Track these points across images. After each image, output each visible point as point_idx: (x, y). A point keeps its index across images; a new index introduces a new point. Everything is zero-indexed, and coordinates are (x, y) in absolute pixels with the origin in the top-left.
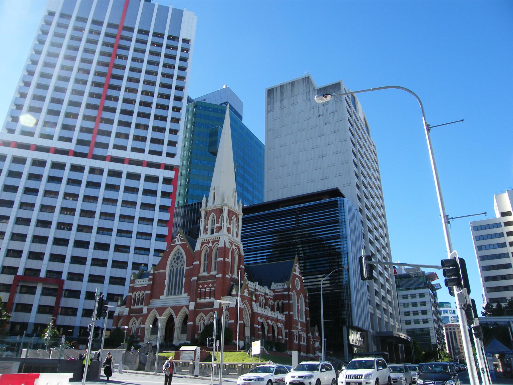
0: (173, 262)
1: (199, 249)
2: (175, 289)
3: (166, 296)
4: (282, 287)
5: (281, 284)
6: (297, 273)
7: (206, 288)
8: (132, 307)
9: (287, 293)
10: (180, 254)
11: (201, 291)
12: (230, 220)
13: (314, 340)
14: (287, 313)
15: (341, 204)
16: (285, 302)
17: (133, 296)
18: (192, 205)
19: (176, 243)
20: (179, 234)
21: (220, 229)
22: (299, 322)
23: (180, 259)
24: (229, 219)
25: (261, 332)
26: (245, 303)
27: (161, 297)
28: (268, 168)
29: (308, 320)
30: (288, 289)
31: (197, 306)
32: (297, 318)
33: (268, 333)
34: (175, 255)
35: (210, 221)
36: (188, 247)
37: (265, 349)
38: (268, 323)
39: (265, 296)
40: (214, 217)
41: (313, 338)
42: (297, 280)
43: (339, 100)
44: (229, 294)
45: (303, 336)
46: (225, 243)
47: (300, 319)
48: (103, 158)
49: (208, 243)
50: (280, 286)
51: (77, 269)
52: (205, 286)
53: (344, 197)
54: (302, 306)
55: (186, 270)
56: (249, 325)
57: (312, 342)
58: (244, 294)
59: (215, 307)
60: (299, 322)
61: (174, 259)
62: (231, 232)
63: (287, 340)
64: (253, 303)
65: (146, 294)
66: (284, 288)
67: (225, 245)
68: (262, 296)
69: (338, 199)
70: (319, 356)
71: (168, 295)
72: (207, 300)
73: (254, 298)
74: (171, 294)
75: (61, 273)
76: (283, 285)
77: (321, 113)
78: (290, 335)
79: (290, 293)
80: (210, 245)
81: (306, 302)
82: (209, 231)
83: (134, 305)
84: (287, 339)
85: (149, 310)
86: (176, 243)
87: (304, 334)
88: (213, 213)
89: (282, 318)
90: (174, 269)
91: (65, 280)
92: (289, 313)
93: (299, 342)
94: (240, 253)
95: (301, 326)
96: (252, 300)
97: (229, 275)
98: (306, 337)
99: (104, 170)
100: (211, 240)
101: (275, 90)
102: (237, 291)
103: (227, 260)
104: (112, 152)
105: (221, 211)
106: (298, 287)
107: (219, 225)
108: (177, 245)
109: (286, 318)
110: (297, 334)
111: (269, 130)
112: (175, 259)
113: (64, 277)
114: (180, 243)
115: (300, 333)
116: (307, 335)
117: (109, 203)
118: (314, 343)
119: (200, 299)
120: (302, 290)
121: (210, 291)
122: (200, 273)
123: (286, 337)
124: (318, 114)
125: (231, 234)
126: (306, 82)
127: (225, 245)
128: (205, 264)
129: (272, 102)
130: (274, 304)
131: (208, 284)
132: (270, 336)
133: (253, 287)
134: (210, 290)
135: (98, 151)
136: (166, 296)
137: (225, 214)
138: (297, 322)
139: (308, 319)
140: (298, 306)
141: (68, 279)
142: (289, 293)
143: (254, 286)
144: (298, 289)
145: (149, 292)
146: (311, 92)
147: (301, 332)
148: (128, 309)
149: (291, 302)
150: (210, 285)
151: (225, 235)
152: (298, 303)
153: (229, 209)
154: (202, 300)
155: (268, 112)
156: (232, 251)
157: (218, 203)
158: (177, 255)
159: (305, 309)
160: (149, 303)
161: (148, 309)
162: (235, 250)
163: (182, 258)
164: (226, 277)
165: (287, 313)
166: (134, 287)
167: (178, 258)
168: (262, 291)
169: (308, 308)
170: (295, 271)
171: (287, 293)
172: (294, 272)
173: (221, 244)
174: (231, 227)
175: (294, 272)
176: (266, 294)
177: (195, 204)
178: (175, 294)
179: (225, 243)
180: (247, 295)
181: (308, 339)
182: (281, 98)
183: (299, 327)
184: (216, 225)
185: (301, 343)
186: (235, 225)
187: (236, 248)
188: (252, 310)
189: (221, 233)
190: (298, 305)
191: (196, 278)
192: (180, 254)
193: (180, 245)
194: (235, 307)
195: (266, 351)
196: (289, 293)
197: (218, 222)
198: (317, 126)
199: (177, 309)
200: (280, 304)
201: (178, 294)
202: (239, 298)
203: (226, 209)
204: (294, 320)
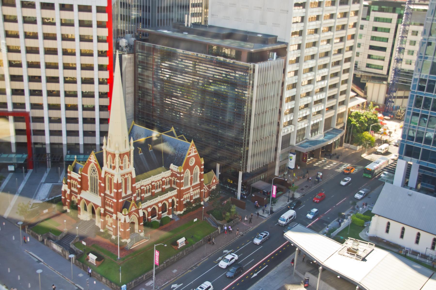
12: (122, 160)
24: (121, 160)
34: (92, 167)
46: (117, 180)
51: (36, 100)
67: (117, 182)
80: (110, 176)
82: (109, 166)
84: (178, 205)
86: (92, 161)
102: (125, 213)
113: (28, 109)
123: (177, 203)
127: (117, 182)
128: (108, 185)
130: (171, 179)
137: (117, 159)
140: (191, 177)
167: (94, 171)
174: (123, 165)
179: (117, 180)
180: (135, 209)
186: (127, 159)
188: (139, 215)
197: (113, 163)
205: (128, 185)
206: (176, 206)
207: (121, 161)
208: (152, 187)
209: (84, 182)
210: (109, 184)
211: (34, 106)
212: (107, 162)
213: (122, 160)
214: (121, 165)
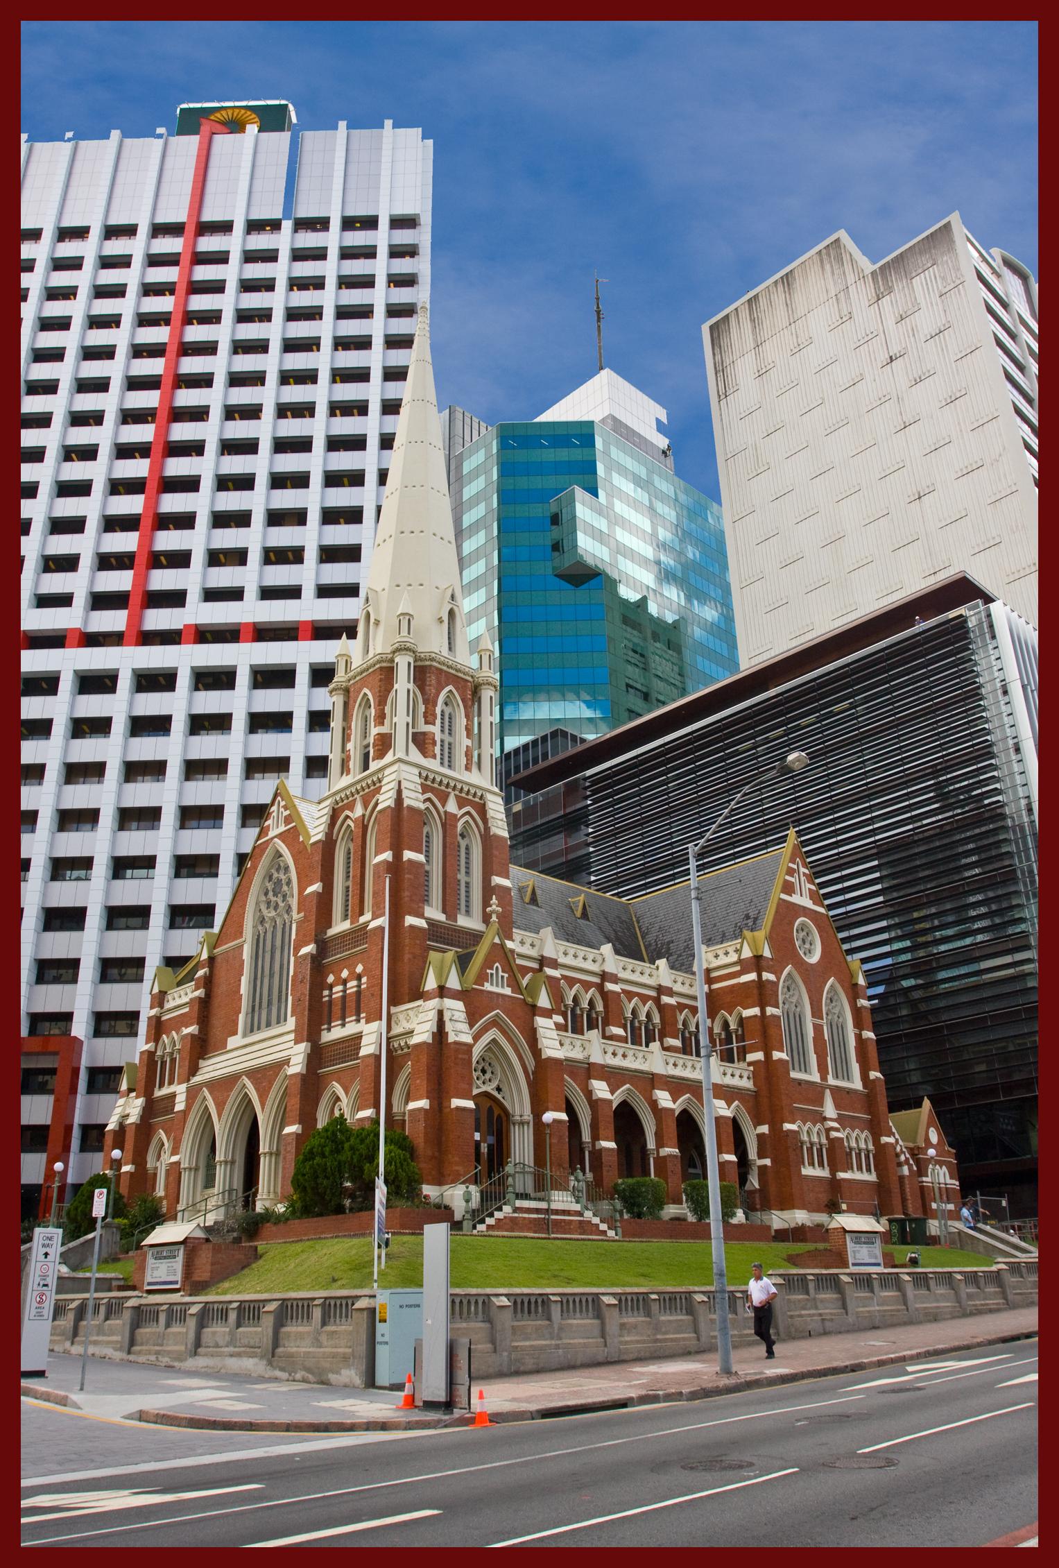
0: (263, 907)
1: (320, 837)
2: (270, 1003)
3: (245, 1036)
4: (733, 957)
5: (731, 945)
6: (802, 899)
7: (345, 982)
8: (158, 1093)
9: (752, 976)
10: (282, 872)
11: (330, 996)
13: (917, 1162)
14: (759, 1056)
15: (980, 624)
16: (747, 1013)
17: (159, 1053)
18: (517, 751)
19: (271, 834)
20: (279, 798)
21: (385, 743)
22: (828, 1092)
23: (285, 888)
24: (426, 702)
25: (612, 1145)
26: (494, 1023)
27: (233, 1042)
28: (741, 582)
29: (874, 1081)
30: (757, 963)
31: (317, 1056)
32: (815, 1077)
33: (660, 1144)
35: (356, 725)
36: (301, 839)
37: (588, 1214)
38: (654, 1104)
39: (657, 1001)
40: (370, 707)
41: (911, 1150)
42: (803, 927)
43: (953, 285)
44: (418, 994)
45: (846, 1144)
46: (399, 792)
47: (830, 1077)
48: (169, 637)
49: (351, 807)
50: (727, 953)
51: (118, 997)
52: (345, 974)
53: (988, 599)
54: (843, 1028)
55: (300, 924)
56: (528, 1115)
57: (910, 1169)
58: (488, 987)
59: (363, 1052)
60: (828, 1092)
61: (266, 894)
62: (437, 750)
63: (765, 1166)
64: (540, 1021)
65: (184, 1038)
66: (740, 962)
67: (399, 799)
68: (645, 999)
69: (970, 612)
70: (845, 1231)
71: (252, 1031)
72: (351, 1028)
73: (544, 1001)
74: (259, 1029)
75: (67, 1017)
76: (736, 951)
77: (894, 350)
78: (778, 1145)
79: (767, 976)
81: (857, 1012)
82: (356, 763)
83: (161, 1085)
84: (767, 1162)
85: (192, 1094)
87: (859, 1139)
88: (366, 690)
89: (736, 1082)
90: (265, 933)
91: (82, 1038)
92: (768, 1056)
93: (833, 1171)
94: (487, 829)
95: (837, 1107)
96: (534, 1010)
97: (420, 915)
98: (871, 1147)
99: (176, 675)
100: (361, 793)
101: (733, 320)
102: (442, 975)
103: (408, 855)
104: (198, 612)
105: (386, 674)
106: (809, 952)
107: (384, 729)
108: (272, 839)
109: (755, 1076)
110: (824, 1141)
111: (729, 456)
112: (271, 894)
113: (80, 1028)
114: (282, 828)
115: (834, 1134)
116: (876, 1142)
117: (207, 777)
118: (921, 1172)
119: (329, 1030)
120: (833, 963)
121: (359, 993)
122: (330, 927)
123: (761, 1156)
124: (887, 356)
125: (434, 757)
126: (831, 262)
127: (399, 799)
129: (727, 361)
131: (349, 963)
132: (665, 1157)
133: (595, 968)
134: (359, 986)
135: (157, 619)
136: (245, 1036)
137: (403, 684)
138: (814, 1093)
139: (875, 1075)
140: (818, 1029)
141: (98, 1033)
142: (760, 976)
143: (599, 959)
144: (815, 958)
145: (193, 1029)
146: (852, 289)
147: (837, 1130)
148: (140, 1101)
149: (770, 1011)
150: (359, 969)
151: (400, 760)
152: (817, 1013)
153: (419, 663)
154: (335, 1033)
155: (719, 396)
156: (444, 825)
157: (380, 644)
158: (276, 875)
159: (859, 1037)
160: (194, 1070)
161: (188, 1090)
162: (467, 818)
163: (289, 883)
164: (407, 924)
165: (759, 1056)
166: (164, 1018)
168: (645, 979)
169: (869, 1035)
170: (788, 888)
171: (752, 976)
172: (784, 896)
173: (386, 800)
174: (435, 729)
175: (784, 896)
176: (661, 990)
177: (526, 747)
178: (268, 1025)
179: (399, 792)
180: (507, 991)
181: (882, 1158)
182: (755, 340)
183: (830, 1110)
184: (374, 731)
185: (842, 1175)
186: (461, 721)
187: (468, 813)
188: (536, 1051)
189: (389, 757)
190: (819, 1021)
191: (309, 949)
192: (282, 872)
193: (280, 836)
194: (430, 1041)
195: (596, 1220)
196: (760, 976)
197: (381, 718)
198: (886, 398)
199: (264, 1075)
200: (733, 1026)
201: (278, 1022)
202: (455, 1008)
203: (403, 663)
204: (800, 1082)
205: (462, 877)
206: (763, 1169)
207: (422, 708)
208: (606, 1006)
209: (221, 989)
210: (350, 883)
211: (109, 1023)
212: (350, 746)
213: (430, 702)
214: (423, 727)
